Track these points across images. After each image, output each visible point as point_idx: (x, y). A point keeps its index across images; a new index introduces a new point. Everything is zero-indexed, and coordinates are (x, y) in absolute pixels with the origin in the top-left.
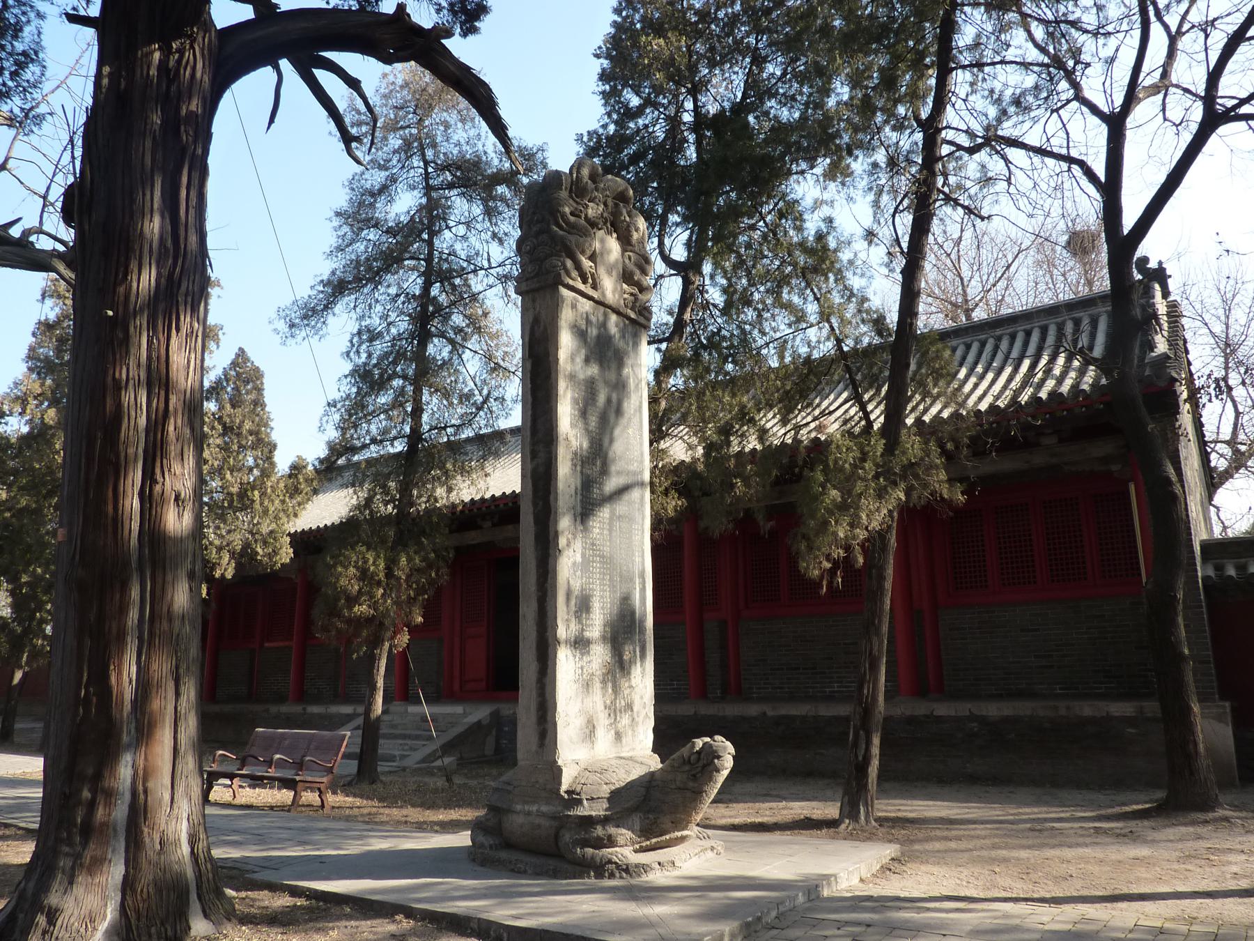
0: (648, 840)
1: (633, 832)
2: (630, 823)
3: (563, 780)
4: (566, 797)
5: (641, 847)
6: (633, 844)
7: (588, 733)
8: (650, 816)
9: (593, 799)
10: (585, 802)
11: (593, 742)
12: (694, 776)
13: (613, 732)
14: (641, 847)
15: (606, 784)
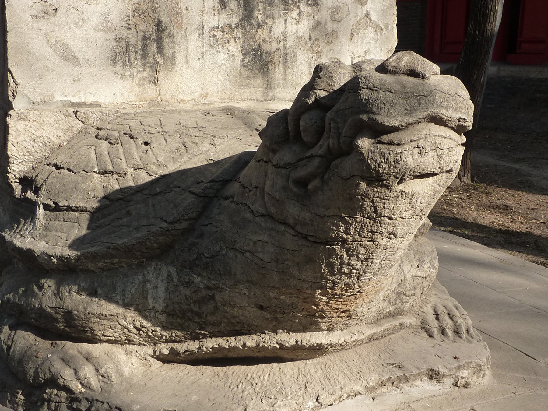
0: (195, 337)
1: (143, 312)
2: (132, 290)
3: (12, 151)
4: (18, 191)
5: (173, 351)
6: (153, 341)
7: (134, 38)
8: (197, 280)
9: (57, 208)
10: (41, 212)
11: (155, 67)
12: (303, 183)
13: (235, 48)
14: (173, 351)
15: (104, 173)
